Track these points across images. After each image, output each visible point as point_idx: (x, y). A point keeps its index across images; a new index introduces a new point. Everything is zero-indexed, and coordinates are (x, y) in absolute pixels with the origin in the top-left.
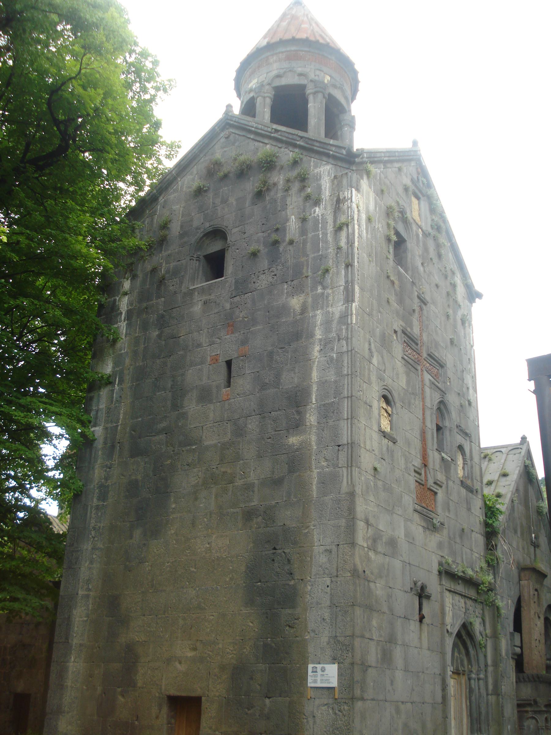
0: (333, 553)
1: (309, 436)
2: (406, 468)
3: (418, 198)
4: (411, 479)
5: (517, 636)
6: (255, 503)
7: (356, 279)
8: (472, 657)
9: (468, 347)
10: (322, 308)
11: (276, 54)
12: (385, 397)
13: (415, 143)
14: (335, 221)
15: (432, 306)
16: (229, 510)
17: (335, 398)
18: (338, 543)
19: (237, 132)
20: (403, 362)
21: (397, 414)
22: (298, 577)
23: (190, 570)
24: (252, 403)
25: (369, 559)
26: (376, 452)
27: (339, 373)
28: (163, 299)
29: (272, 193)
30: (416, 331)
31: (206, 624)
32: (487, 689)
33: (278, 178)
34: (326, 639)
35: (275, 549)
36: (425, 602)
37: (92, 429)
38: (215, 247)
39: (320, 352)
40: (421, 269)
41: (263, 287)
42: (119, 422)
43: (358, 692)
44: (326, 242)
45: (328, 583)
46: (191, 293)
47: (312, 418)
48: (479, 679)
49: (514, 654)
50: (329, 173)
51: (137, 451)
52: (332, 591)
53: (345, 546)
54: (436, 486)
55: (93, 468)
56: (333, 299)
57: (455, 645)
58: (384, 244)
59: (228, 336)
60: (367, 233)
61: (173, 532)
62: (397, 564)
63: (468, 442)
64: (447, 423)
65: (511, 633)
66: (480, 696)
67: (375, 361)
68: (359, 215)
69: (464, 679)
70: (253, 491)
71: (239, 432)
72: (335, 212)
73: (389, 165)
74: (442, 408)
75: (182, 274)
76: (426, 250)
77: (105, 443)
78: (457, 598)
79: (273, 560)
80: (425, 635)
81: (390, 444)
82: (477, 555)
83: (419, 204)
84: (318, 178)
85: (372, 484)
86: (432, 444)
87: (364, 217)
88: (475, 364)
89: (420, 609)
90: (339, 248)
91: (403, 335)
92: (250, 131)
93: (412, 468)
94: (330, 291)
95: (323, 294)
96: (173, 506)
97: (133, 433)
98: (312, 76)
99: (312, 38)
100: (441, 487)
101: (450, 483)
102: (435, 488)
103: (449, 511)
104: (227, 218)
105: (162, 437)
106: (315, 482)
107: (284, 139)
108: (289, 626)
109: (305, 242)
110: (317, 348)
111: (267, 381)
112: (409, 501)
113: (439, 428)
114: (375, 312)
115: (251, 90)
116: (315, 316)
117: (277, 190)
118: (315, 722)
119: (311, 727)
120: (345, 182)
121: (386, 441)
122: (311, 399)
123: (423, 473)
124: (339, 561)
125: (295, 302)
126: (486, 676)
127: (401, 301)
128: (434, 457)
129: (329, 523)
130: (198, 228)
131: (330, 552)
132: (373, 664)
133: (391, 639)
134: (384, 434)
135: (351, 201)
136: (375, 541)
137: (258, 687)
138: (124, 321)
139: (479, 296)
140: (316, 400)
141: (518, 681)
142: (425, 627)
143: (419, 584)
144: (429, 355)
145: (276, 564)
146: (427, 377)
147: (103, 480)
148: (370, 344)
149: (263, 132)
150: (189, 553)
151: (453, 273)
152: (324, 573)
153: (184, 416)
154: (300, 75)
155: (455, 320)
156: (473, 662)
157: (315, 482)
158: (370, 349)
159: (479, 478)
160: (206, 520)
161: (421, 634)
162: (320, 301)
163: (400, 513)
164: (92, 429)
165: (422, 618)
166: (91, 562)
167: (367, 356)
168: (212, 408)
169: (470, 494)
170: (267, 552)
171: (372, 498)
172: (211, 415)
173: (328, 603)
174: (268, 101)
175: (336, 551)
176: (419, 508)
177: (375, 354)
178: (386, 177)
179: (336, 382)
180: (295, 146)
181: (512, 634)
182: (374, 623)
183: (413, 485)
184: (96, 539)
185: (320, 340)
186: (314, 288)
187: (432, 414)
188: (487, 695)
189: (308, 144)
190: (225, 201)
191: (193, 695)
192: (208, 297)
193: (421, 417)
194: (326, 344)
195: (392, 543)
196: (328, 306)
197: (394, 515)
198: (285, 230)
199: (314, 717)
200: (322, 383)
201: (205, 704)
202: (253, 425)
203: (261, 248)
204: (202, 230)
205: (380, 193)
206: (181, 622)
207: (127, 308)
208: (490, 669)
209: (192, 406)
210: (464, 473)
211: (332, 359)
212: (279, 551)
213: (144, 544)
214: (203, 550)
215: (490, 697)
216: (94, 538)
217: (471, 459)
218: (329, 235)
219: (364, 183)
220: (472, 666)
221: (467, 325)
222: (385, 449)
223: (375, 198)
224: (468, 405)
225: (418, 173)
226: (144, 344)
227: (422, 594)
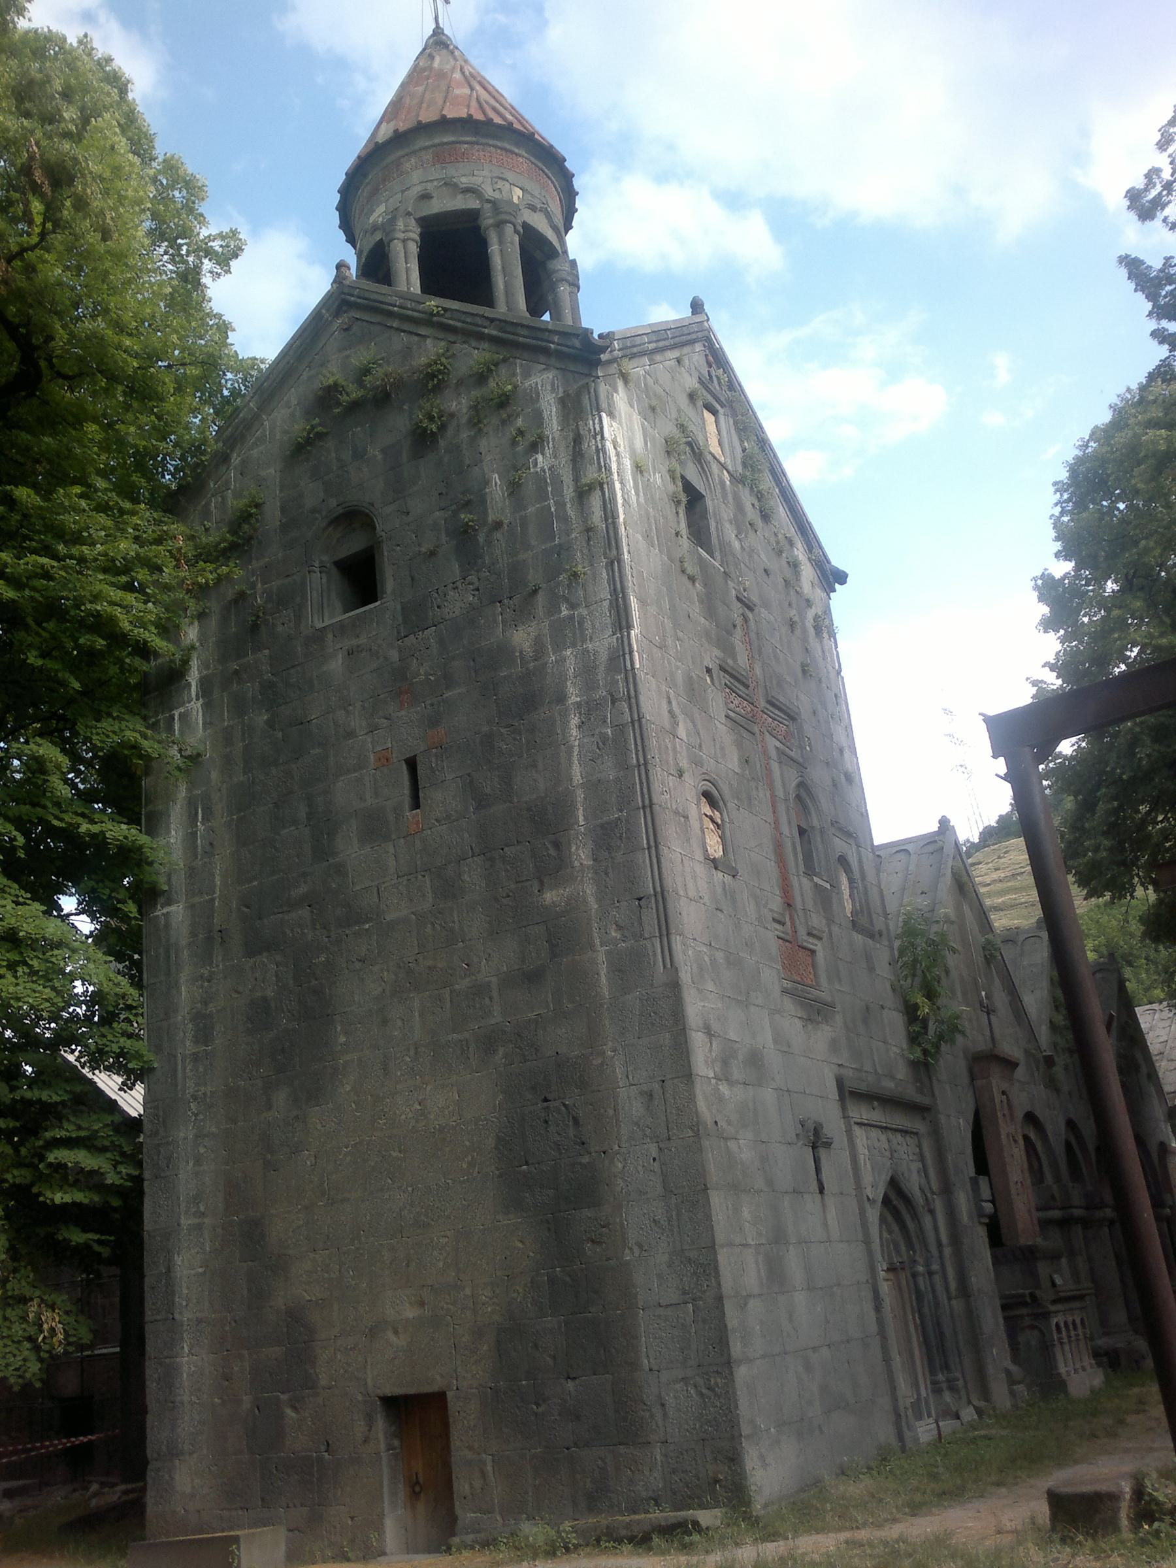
1: (582, 887)
2: (759, 919)
3: (714, 412)
4: (770, 937)
5: (983, 1182)
6: (496, 1018)
7: (630, 584)
8: (913, 1234)
9: (833, 674)
10: (574, 645)
11: (414, 152)
12: (706, 795)
13: (697, 306)
14: (576, 480)
15: (763, 610)
16: (450, 1037)
17: (621, 811)
19: (366, 317)
20: (729, 723)
21: (731, 822)
22: (597, 1148)
24: (466, 835)
25: (721, 1099)
26: (706, 899)
27: (623, 765)
28: (266, 652)
29: (450, 431)
30: (742, 660)
31: (435, 1253)
32: (947, 1289)
33: (459, 404)
35: (546, 1100)
36: (823, 1153)
37: (165, 911)
38: (354, 545)
39: (580, 727)
40: (737, 545)
41: (457, 613)
42: (214, 893)
43: (736, 1348)
44: (565, 519)
45: (654, 1151)
46: (319, 636)
47: (581, 855)
48: (930, 1273)
49: (981, 1213)
50: (553, 385)
51: (256, 945)
53: (675, 1081)
54: (811, 940)
55: (177, 985)
56: (593, 627)
57: (882, 1219)
58: (669, 509)
59: (403, 713)
60: (637, 494)
61: (348, 1088)
62: (768, 1096)
63: (854, 848)
64: (815, 822)
65: (971, 1178)
66: (937, 1304)
67: (682, 732)
68: (619, 463)
69: (902, 1276)
70: (491, 998)
71: (448, 890)
72: (574, 461)
73: (658, 357)
74: (804, 796)
75: (298, 600)
76: (740, 508)
77: (194, 934)
78: (875, 1133)
79: (546, 1122)
80: (832, 1213)
81: (728, 879)
82: (894, 1049)
83: (716, 422)
84: (533, 397)
85: (707, 959)
86: (795, 864)
87: (627, 463)
88: (847, 703)
89: (818, 1170)
90: (589, 530)
91: (722, 673)
92: (390, 314)
93: (769, 916)
94: (585, 612)
95: (571, 617)
96: (342, 1039)
97: (245, 910)
98: (489, 192)
99: (479, 116)
100: (820, 939)
101: (835, 929)
102: (811, 943)
103: (840, 980)
104: (368, 484)
105: (305, 912)
106: (603, 970)
107: (459, 324)
108: (593, 1241)
109: (524, 522)
110: (574, 721)
111: (488, 790)
112: (771, 977)
113: (802, 832)
114: (669, 641)
115: (375, 228)
116: (561, 661)
117: (458, 426)
118: (665, 1415)
119: (660, 1423)
120: (586, 401)
121: (720, 874)
122: (577, 818)
123: (787, 919)
125: (522, 638)
126: (943, 1265)
127: (710, 611)
128: (802, 886)
130: (314, 511)
131: (650, 1096)
132: (756, 1291)
133: (779, 1237)
134: (715, 863)
135: (603, 438)
136: (725, 1063)
137: (550, 1361)
138: (197, 699)
139: (841, 578)
140: (586, 819)
141: (996, 1261)
142: (830, 1202)
143: (810, 1125)
144: (769, 702)
146: (771, 743)
147: (199, 1005)
148: (670, 702)
149: (416, 314)
150: (385, 1124)
151: (791, 543)
153: (340, 870)
154: (467, 190)
155: (804, 631)
156: (917, 1246)
157: (603, 970)
158: (671, 712)
159: (879, 910)
161: (824, 1212)
162: (568, 632)
163: (760, 1001)
164: (165, 911)
165: (821, 1190)
166: (198, 1162)
167: (668, 726)
168: (391, 850)
169: (871, 942)
171: (710, 986)
172: (392, 863)
173: (659, 1188)
174: (413, 248)
176: (789, 985)
177: (681, 718)
178: (656, 382)
179: (617, 780)
180: (481, 337)
181: (974, 1182)
182: (746, 1214)
183: (774, 946)
184: (201, 1117)
185: (579, 705)
186: (553, 608)
187: (788, 808)
188: (950, 1299)
189: (504, 332)
190: (359, 455)
191: (427, 1389)
192: (354, 642)
193: (770, 818)
194: (591, 710)
195: (755, 1060)
196: (584, 641)
197: (752, 1009)
198: (483, 501)
200: (593, 786)
202: (472, 876)
203: (444, 538)
204: (324, 513)
205: (651, 411)
207: (200, 673)
208: (947, 1251)
209: (351, 849)
210: (854, 905)
211: (604, 739)
212: (556, 1104)
213: (297, 1118)
214: (410, 1115)
215: (954, 1302)
216: (196, 1115)
217: (863, 878)
218: (568, 506)
219: (620, 399)
220: (915, 1252)
221: (825, 635)
222: (719, 890)
223: (643, 425)
224: (847, 780)
225: (710, 366)
226: (243, 740)
227: (817, 1140)
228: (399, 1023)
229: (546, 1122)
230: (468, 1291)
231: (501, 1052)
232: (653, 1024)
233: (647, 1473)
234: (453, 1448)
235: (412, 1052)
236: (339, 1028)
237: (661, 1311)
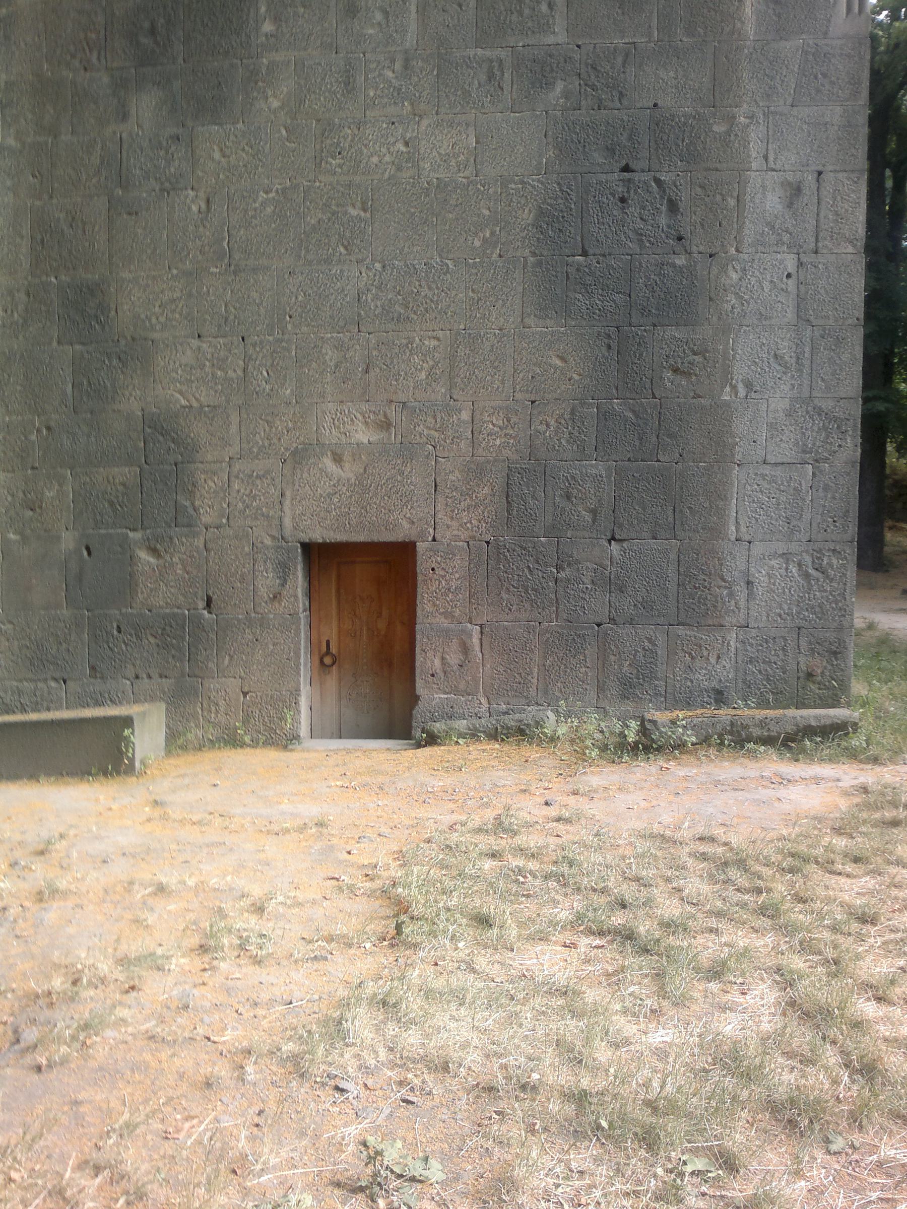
0: (806, 191)
6: (558, 36)
18: (820, 168)
22: (702, 248)
23: (346, 213)
34: (785, 404)
45: (791, 267)
52: (802, 287)
53: (841, 175)
61: (275, 104)
108: (676, 371)
118: (751, 596)
119: (742, 604)
124: (822, 215)
129: (795, 111)
137: (588, 517)
145: (633, 210)
150: (340, 166)
152: (780, 242)
160: (390, 74)
170: (603, 177)
173: (791, 315)
175: (814, 186)
199: (748, 583)
201: (424, 563)
206: (330, 355)
214: (387, 158)
228: (379, 17)
229: (623, 200)
230: (465, 416)
231: (559, 86)
232: (818, 91)
233: (713, 660)
234: (419, 613)
235: (398, 66)
236: (263, 9)
237: (767, 470)
